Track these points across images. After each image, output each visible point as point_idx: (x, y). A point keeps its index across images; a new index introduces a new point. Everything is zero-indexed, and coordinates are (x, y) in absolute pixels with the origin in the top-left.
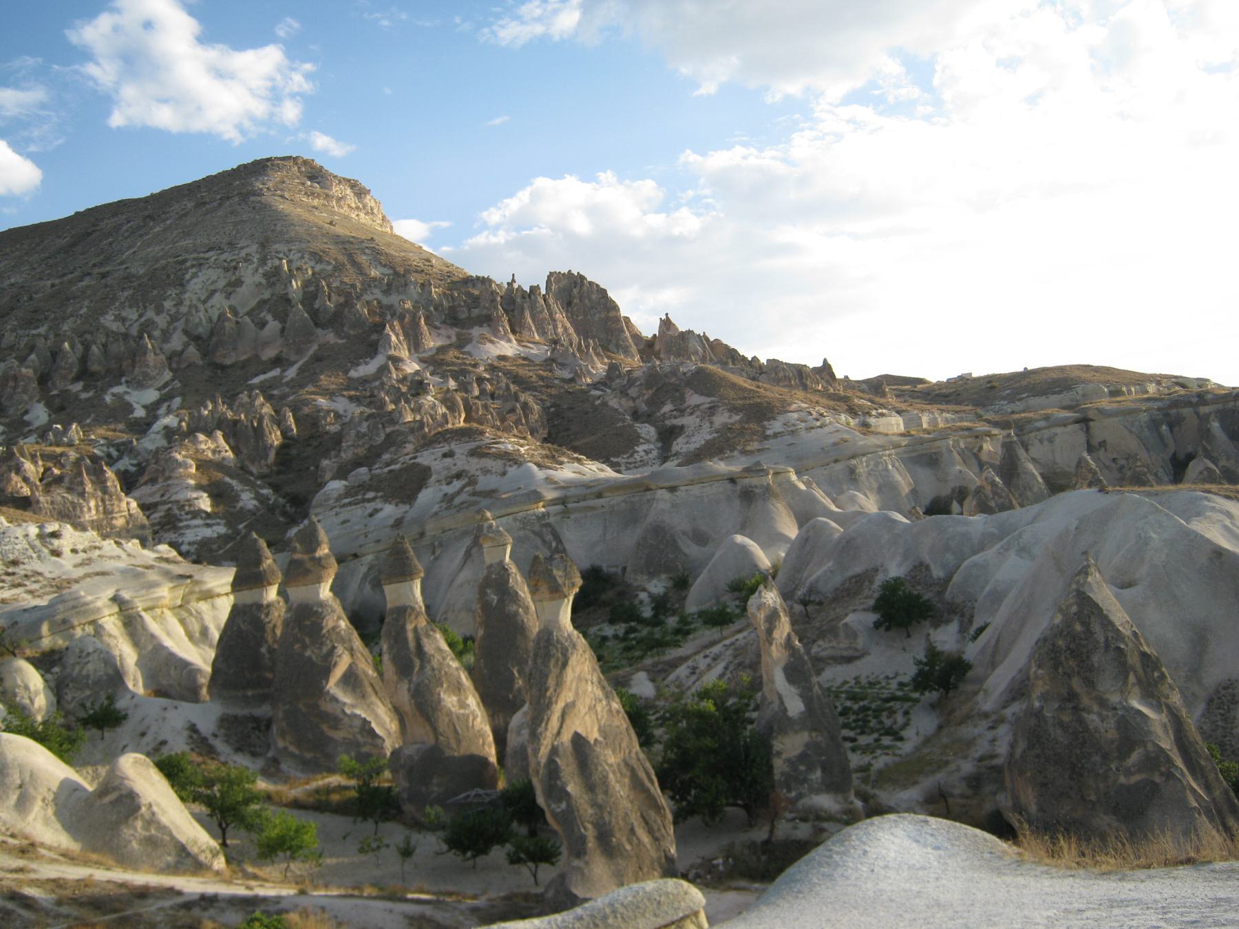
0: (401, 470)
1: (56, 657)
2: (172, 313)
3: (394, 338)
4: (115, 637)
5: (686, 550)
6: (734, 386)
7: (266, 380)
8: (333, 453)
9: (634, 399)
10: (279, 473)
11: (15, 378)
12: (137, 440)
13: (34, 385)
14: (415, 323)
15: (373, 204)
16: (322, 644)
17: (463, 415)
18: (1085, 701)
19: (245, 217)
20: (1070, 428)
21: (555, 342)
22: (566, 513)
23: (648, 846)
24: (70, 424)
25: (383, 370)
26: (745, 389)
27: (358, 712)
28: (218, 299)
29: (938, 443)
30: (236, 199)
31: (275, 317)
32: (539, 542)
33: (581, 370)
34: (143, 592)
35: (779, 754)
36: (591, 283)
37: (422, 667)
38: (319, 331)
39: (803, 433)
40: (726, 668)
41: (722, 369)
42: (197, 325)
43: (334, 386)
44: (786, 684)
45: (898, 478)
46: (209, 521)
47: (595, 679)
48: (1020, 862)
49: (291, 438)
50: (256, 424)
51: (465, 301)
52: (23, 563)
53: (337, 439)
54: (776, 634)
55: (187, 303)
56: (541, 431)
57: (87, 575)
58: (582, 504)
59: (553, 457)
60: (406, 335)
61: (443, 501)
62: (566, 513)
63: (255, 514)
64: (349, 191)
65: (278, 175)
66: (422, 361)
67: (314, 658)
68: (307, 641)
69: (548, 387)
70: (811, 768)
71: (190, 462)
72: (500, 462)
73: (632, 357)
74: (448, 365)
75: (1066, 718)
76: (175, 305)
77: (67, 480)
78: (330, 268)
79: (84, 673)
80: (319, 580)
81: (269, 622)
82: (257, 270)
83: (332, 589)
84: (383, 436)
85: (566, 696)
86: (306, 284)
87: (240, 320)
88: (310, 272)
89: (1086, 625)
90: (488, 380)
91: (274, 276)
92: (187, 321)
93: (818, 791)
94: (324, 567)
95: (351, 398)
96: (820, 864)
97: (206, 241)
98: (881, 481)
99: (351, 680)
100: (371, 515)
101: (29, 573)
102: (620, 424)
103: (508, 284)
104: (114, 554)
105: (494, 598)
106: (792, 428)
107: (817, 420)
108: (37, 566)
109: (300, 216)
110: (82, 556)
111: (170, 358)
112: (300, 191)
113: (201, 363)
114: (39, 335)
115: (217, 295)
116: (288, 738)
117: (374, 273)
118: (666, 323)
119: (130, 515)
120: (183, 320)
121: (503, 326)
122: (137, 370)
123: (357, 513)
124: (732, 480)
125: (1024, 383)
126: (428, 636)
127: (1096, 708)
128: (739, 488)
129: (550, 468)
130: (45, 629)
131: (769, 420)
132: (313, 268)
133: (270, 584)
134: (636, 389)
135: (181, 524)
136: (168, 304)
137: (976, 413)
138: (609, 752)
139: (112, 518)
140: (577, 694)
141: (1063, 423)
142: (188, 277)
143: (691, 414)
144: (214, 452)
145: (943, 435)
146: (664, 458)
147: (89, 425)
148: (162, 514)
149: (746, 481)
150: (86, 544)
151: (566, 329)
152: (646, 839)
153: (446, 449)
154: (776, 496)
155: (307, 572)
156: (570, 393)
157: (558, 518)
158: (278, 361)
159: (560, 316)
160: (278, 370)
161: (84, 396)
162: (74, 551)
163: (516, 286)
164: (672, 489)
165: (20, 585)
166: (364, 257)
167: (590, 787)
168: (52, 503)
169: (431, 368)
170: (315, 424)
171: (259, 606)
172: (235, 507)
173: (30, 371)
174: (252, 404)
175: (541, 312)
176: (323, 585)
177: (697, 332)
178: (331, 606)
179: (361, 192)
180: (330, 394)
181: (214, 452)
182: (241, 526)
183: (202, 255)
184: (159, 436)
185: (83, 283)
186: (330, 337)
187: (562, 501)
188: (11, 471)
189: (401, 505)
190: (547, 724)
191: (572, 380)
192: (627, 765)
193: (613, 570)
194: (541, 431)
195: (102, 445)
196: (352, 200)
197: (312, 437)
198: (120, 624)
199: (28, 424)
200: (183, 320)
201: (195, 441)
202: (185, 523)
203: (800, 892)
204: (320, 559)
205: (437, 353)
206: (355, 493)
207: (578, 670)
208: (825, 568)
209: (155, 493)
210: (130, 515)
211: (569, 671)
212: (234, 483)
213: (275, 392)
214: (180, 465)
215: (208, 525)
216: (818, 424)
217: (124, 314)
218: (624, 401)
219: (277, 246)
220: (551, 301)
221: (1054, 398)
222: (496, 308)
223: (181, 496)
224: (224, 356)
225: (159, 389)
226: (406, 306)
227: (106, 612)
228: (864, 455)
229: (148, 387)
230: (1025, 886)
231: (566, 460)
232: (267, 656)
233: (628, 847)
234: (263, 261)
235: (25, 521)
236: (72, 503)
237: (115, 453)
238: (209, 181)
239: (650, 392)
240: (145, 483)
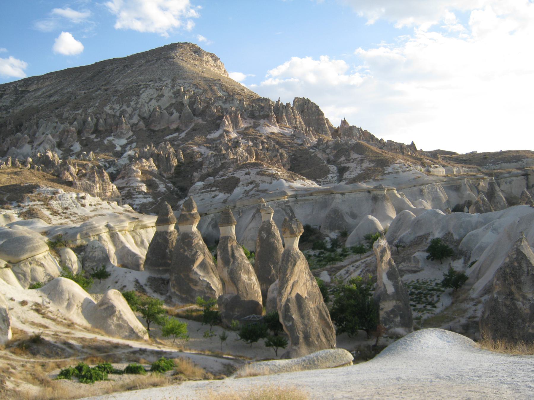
0: (227, 179)
1: (83, 248)
2: (134, 107)
3: (227, 122)
4: (107, 242)
5: (347, 220)
6: (372, 151)
7: (172, 138)
8: (199, 170)
9: (328, 154)
10: (176, 177)
11: (68, 131)
12: (117, 160)
13: (76, 135)
14: (236, 117)
15: (221, 65)
16: (192, 250)
17: (255, 157)
18: (517, 296)
19: (166, 68)
20: (519, 178)
21: (296, 128)
22: (296, 201)
23: (325, 343)
24: (90, 152)
25: (222, 136)
26: (377, 153)
27: (205, 279)
28: (153, 102)
29: (460, 181)
30: (163, 60)
32: (284, 213)
33: (306, 140)
34: (118, 224)
35: (382, 309)
36: (312, 103)
37: (234, 262)
38: (195, 118)
39: (401, 173)
40: (361, 272)
41: (367, 143)
42: (144, 113)
43: (200, 142)
44: (387, 280)
45: (441, 195)
46: (145, 196)
47: (307, 272)
48: (481, 349)
49: (181, 163)
50: (167, 156)
51: (258, 108)
52: (70, 209)
53: (201, 164)
54: (384, 258)
55: (140, 103)
56: (287, 166)
57: (96, 215)
58: (303, 198)
59: (292, 177)
60: (232, 122)
61: (244, 193)
62: (296, 201)
63: (165, 194)
64: (210, 59)
65: (181, 50)
66: (238, 133)
67: (188, 255)
68: (186, 248)
69: (291, 147)
70: (396, 316)
71: (139, 170)
72: (269, 178)
73: (329, 136)
74: (249, 135)
75: (508, 303)
76: (135, 104)
77: (88, 175)
78: (201, 91)
79: (94, 255)
80: (192, 223)
81: (170, 240)
82: (170, 90)
83: (197, 227)
84: (220, 164)
85: (294, 278)
86: (191, 97)
87: (162, 111)
88: (193, 93)
89: (520, 263)
90: (266, 142)
91: (177, 94)
92: (140, 111)
93: (398, 326)
94: (195, 218)
95: (207, 147)
96: (402, 344)
97: (150, 77)
98: (434, 196)
99: (203, 265)
100: (213, 197)
101: (72, 213)
102: (322, 165)
104: (107, 207)
105: (265, 235)
106: (396, 171)
107: (407, 168)
108: (75, 210)
109: (189, 68)
110: (94, 207)
111: (132, 126)
112: (190, 57)
113: (145, 129)
114: (78, 114)
115: (153, 100)
116: (176, 288)
117: (220, 94)
118: (344, 122)
119: (113, 191)
120: (138, 111)
121: (274, 120)
122: (118, 130)
123: (208, 196)
124: (369, 192)
125: (500, 157)
126: (237, 249)
127: (521, 299)
128: (371, 195)
129: (290, 182)
130: (78, 236)
131: (386, 166)
132: (194, 91)
133: (172, 224)
134: (330, 150)
135: (134, 196)
136: (132, 103)
137: (478, 169)
138: (311, 303)
139: (106, 192)
140: (299, 277)
141: (517, 176)
142: (141, 92)
143: (353, 162)
144: (149, 167)
145: (463, 177)
146: (340, 181)
147: (97, 153)
148: (126, 192)
149: (375, 193)
150: (96, 203)
151: (300, 122)
152: (324, 340)
153: (247, 171)
154: (387, 200)
155: (188, 219)
156: (301, 150)
157: (293, 203)
158: (177, 130)
159: (298, 117)
160: (177, 133)
161: (96, 140)
162: (91, 205)
163: (280, 103)
164: (343, 194)
165: (68, 218)
166: (216, 87)
167: (302, 317)
168: (82, 184)
169: (242, 136)
170: (192, 157)
171: (167, 233)
172: (156, 191)
173: (74, 129)
174: (166, 148)
175: (290, 115)
176: (194, 225)
177: (357, 127)
178: (196, 235)
179: (215, 59)
180: (199, 145)
181: (149, 167)
182: (159, 199)
183: (147, 83)
184: (126, 159)
185: (98, 93)
186: (200, 121)
187: (295, 196)
188: (65, 170)
189: (226, 194)
190: (286, 289)
191: (302, 145)
192: (318, 308)
193: (315, 227)
194: (287, 166)
195: (102, 161)
196: (212, 62)
197: (190, 163)
198: (109, 236)
199: (72, 151)
200: (138, 111)
201: (141, 162)
202: (136, 196)
203: (393, 353)
204: (193, 214)
205: (245, 130)
206: (207, 188)
207: (300, 268)
208: (407, 232)
209: (123, 183)
210: (113, 191)
211: (296, 268)
212: (157, 180)
213: (176, 143)
214: (135, 171)
215: (145, 198)
216: (408, 169)
217: (114, 106)
218: (324, 154)
219: (179, 81)
220: (295, 110)
221: (513, 164)
222: (271, 112)
223: (134, 185)
224: (155, 127)
225: (127, 139)
226: (233, 109)
227: (104, 231)
228: (427, 184)
229: (123, 138)
230: (482, 356)
231: (298, 179)
232: (169, 253)
233: (316, 343)
234: (173, 87)
235: (71, 191)
236: (90, 185)
237: (107, 165)
238: (152, 52)
239: (335, 151)
240: (120, 178)
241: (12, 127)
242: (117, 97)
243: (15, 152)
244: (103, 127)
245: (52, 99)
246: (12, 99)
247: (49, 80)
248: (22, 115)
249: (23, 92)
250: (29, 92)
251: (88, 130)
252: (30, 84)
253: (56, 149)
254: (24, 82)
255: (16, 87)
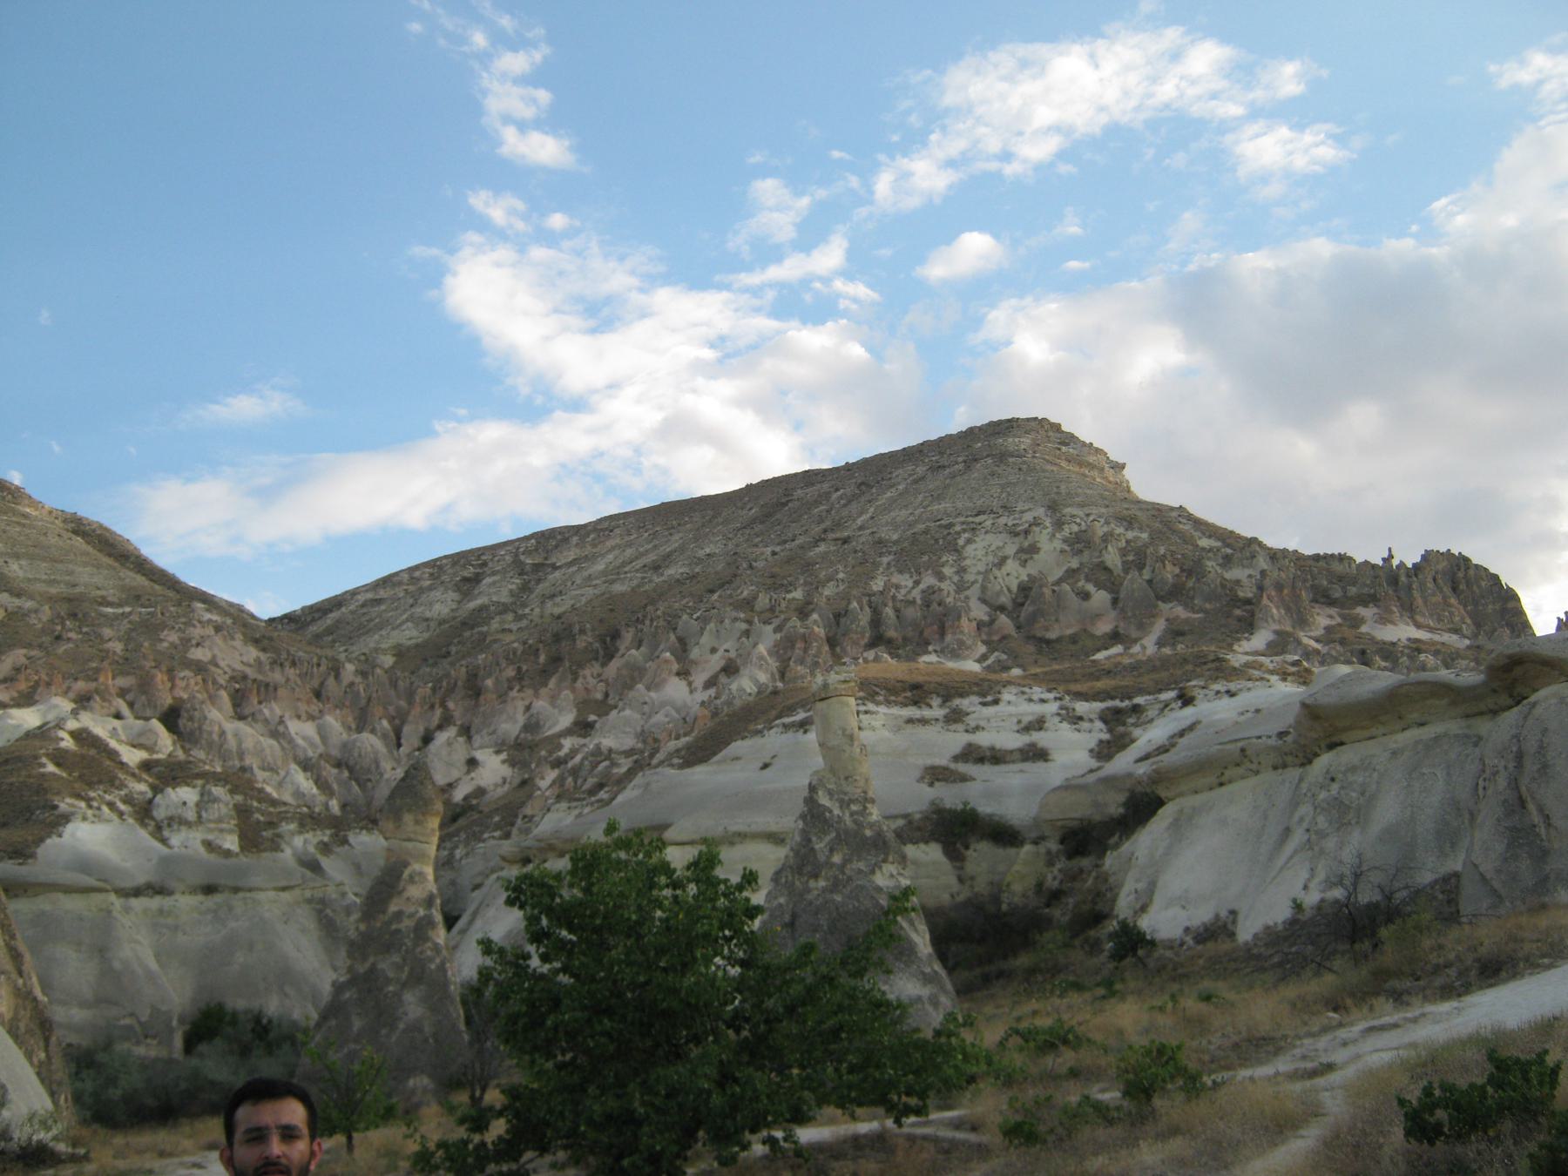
14: (1296, 597)
19: (1013, 479)
28: (1011, 566)
31: (1099, 586)
36: (1476, 566)
42: (998, 594)
76: (957, 573)
82: (1054, 535)
103: (1384, 559)
113: (1016, 635)
115: (1009, 562)
142: (961, 542)
163: (1395, 562)
183: (971, 519)
185: (817, 550)
219: (1068, 510)
224: (1047, 629)
225: (978, 661)
234: (1059, 525)
241: (590, 640)
242: (891, 557)
243: (647, 699)
244: (896, 630)
245: (671, 572)
246: (514, 587)
247: (617, 531)
248: (612, 610)
249: (537, 567)
250: (555, 567)
251: (855, 636)
252: (556, 547)
254: (538, 543)
255: (517, 555)
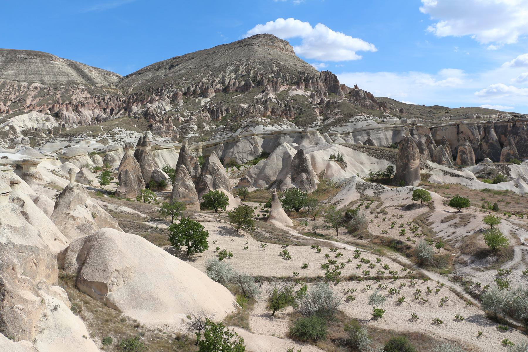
3: (269, 88)
167: (126, 176)
253: (169, 105)
